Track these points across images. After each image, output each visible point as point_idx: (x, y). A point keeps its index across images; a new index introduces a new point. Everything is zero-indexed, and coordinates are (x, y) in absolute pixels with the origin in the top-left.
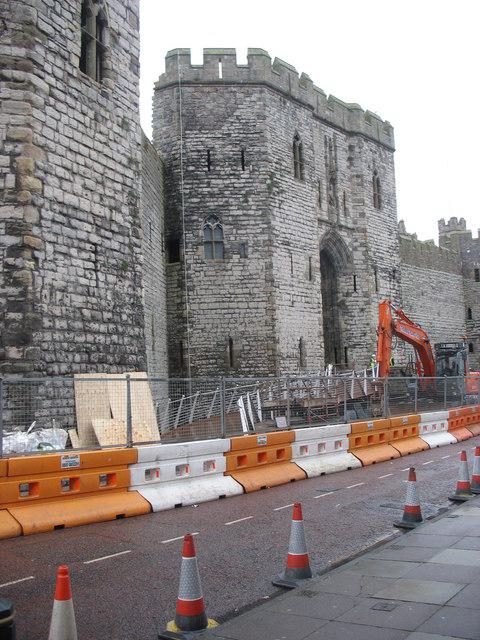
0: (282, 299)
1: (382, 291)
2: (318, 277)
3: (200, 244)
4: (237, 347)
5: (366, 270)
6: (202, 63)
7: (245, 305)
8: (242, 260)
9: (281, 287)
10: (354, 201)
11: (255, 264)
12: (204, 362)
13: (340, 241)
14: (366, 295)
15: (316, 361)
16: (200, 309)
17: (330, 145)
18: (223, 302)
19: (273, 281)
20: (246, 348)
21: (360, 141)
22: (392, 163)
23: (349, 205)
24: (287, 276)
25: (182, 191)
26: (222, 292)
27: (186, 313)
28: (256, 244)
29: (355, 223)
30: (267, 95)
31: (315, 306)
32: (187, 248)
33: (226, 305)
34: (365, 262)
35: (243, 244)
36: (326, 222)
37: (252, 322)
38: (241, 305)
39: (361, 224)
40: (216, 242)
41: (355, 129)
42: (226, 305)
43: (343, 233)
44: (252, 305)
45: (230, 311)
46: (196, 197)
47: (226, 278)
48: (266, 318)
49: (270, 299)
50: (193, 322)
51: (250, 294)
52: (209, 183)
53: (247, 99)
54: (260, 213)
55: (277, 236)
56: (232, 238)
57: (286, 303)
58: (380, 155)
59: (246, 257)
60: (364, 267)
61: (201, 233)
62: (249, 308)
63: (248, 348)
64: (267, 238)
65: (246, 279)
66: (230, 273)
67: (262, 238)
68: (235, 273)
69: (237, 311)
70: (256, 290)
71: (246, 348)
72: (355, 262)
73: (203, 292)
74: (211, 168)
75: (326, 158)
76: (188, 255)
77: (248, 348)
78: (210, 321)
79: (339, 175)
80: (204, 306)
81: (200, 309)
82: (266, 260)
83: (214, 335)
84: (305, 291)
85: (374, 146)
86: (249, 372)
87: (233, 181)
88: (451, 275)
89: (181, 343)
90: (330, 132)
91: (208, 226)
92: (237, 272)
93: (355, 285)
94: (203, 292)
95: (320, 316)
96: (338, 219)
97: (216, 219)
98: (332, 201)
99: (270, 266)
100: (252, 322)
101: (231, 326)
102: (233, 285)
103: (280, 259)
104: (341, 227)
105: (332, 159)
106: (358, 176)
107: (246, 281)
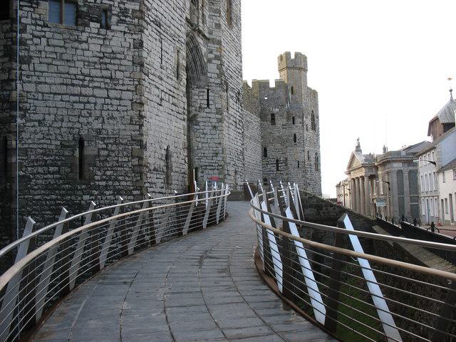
0: (151, 94)
1: (231, 111)
4: (90, 151)
7: (104, 93)
8: (103, 31)
9: (151, 76)
10: (211, 9)
11: (119, 40)
12: (40, 170)
14: (219, 111)
16: (37, 92)
18: (73, 85)
19: (142, 65)
23: (207, 13)
24: (157, 65)
26: (73, 71)
28: (124, 12)
29: (210, 33)
31: (181, 110)
33: (77, 90)
35: (105, 11)
37: (112, 118)
38: (97, 92)
42: (77, 90)
43: (200, 40)
44: (113, 94)
45: (82, 99)
47: (79, 52)
48: (131, 113)
49: (138, 88)
50: (27, 110)
51: (111, 78)
55: (148, 9)
60: (218, 81)
62: (108, 97)
63: (106, 153)
64: (137, 8)
65: (106, 58)
66: (84, 46)
68: (92, 47)
70: (119, 75)
72: (209, 75)
73: (44, 68)
77: (106, 153)
78: (53, 111)
80: (45, 88)
81: (37, 92)
82: (135, 37)
83: (58, 131)
84: (172, 89)
86: (106, 187)
89: (6, 140)
93: (208, 100)
94: (44, 68)
95: (185, 124)
100: (112, 118)
101: (82, 120)
104: (200, 32)
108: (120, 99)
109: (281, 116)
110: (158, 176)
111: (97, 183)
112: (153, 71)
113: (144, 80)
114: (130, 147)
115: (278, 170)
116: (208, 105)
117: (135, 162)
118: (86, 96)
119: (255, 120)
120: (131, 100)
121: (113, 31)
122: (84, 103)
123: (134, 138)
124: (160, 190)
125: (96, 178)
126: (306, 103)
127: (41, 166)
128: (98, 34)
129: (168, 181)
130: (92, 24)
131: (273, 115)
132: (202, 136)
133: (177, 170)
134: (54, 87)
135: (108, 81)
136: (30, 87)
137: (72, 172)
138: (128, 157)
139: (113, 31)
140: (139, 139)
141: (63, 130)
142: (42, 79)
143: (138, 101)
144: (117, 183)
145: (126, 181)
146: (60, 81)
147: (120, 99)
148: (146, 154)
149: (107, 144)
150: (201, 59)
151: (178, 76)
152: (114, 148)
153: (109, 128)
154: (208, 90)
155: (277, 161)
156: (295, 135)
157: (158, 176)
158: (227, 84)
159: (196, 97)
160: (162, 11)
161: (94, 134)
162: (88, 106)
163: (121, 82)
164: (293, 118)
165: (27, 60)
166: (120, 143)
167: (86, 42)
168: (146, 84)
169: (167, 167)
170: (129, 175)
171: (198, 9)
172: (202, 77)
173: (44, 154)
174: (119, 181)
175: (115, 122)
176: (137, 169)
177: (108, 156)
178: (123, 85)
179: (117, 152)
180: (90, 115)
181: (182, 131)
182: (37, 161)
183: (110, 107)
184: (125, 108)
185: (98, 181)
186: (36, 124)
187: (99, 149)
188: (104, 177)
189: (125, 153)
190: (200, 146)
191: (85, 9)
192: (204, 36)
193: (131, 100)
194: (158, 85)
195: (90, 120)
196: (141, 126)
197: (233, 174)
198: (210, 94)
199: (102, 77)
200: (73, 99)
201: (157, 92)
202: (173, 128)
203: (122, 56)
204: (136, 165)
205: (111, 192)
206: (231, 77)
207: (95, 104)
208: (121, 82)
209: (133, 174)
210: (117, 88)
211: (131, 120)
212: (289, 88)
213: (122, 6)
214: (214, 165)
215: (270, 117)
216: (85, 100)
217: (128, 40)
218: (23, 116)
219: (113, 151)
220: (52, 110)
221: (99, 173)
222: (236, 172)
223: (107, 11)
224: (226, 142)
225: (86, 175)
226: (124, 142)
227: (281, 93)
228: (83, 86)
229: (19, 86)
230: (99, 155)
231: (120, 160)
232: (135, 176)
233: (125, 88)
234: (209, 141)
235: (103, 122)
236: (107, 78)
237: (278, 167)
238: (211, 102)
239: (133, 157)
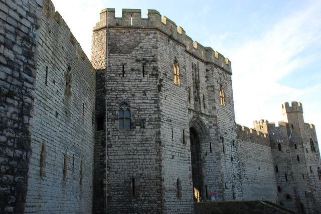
0: (166, 154)
1: (227, 152)
2: (188, 142)
3: (117, 119)
4: (137, 184)
5: (217, 140)
6: (121, 17)
7: (143, 157)
10: (209, 100)
11: (149, 132)
12: (116, 193)
13: (201, 122)
17: (195, 68)
18: (129, 155)
20: (143, 184)
21: (212, 67)
22: (231, 81)
23: (207, 102)
24: (170, 140)
25: (107, 88)
26: (129, 149)
27: (106, 161)
29: (210, 112)
30: (159, 35)
31: (187, 159)
32: (108, 121)
33: (131, 157)
34: (216, 135)
35: (143, 120)
36: (193, 110)
39: (213, 113)
40: (126, 119)
41: (209, 60)
42: (131, 157)
43: (203, 118)
44: (147, 157)
46: (115, 91)
49: (159, 154)
50: (110, 167)
51: (146, 150)
52: (123, 84)
53: (147, 37)
54: (153, 101)
55: (163, 116)
56: (136, 116)
57: (168, 156)
58: (224, 76)
59: (144, 128)
60: (216, 138)
61: (117, 113)
63: (144, 184)
64: (157, 116)
66: (134, 137)
67: (154, 116)
68: (137, 137)
69: (138, 160)
70: (150, 148)
71: (143, 184)
73: (117, 149)
74: (125, 75)
75: (193, 75)
76: (109, 126)
77: (144, 184)
78: (121, 167)
79: (201, 85)
80: (117, 157)
82: (156, 130)
84: (180, 149)
85: (220, 71)
87: (137, 83)
88: (265, 147)
90: (195, 61)
91: (122, 109)
92: (138, 137)
93: (211, 149)
94: (117, 149)
95: (190, 165)
96: (200, 109)
97: (127, 104)
98: (197, 99)
99: (159, 133)
101: (133, 170)
102: (136, 145)
103: (165, 130)
104: (202, 114)
105: (196, 75)
106: (211, 86)
107: (144, 142)
109: (285, 144)
112: (167, 144)
116: (211, 151)
117: (158, 187)
120: (156, 159)
121: (146, 129)
122: (135, 162)
124: (174, 200)
126: (303, 134)
127: (116, 191)
128: (140, 131)
129: (179, 195)
130: (137, 127)
131: (279, 145)
134: (122, 157)
136: (112, 157)
137: (129, 193)
139: (146, 129)
140: (160, 176)
141: (126, 175)
142: (116, 154)
146: (123, 153)
148: (163, 183)
150: (205, 127)
151: (184, 142)
154: (210, 143)
155: (286, 174)
156: (298, 156)
159: (204, 148)
160: (171, 114)
163: (151, 151)
164: (295, 145)
165: (110, 146)
167: (135, 135)
168: (163, 150)
171: (200, 102)
173: (117, 186)
178: (152, 152)
181: (188, 169)
182: (114, 189)
186: (114, 173)
191: (133, 121)
192: (205, 115)
193: (156, 159)
196: (161, 170)
197: (231, 188)
200: (130, 161)
201: (170, 153)
202: (181, 169)
203: (151, 140)
206: (226, 133)
208: (151, 151)
212: (290, 125)
213: (150, 117)
215: (277, 145)
217: (153, 132)
218: (109, 170)
220: (121, 167)
223: (143, 120)
224: (223, 170)
227: (285, 131)
228: (135, 155)
229: (107, 158)
233: (153, 154)
239: (157, 185)
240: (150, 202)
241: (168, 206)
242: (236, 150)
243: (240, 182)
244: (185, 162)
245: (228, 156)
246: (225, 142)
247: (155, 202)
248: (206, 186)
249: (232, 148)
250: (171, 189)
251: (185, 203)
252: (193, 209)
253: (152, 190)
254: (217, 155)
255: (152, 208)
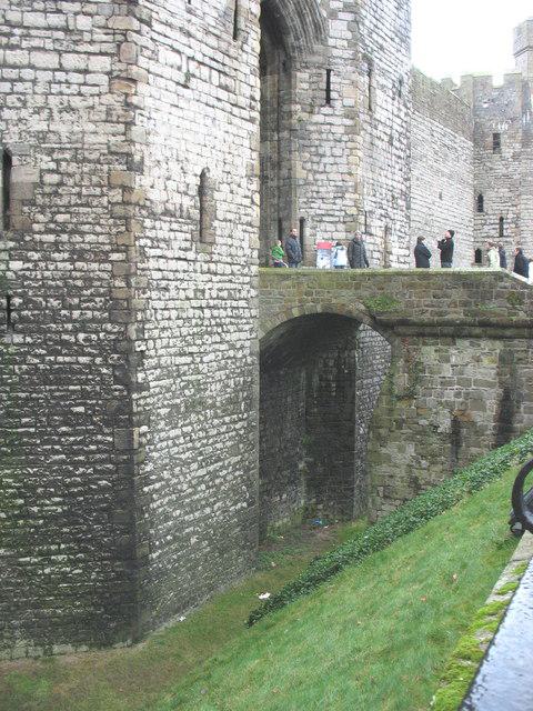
7: (51, 60)
9: (156, 26)
15: (238, 233)
20: (49, 178)
31: (243, 101)
34: (352, 44)
37: (70, 109)
38: (39, 59)
44: (70, 61)
48: (108, 99)
51: (66, 30)
57: (168, 72)
63: (55, 178)
69: (28, 74)
71: (49, 178)
72: (331, 42)
77: (55, 178)
84: (219, 57)
86: (56, 246)
93: (328, 90)
95: (255, 128)
100: (70, 109)
108: (86, 72)
110: (175, 226)
111: (37, 237)
112: (164, 16)
113: (138, 32)
114: (106, 167)
115: (501, 235)
117: (116, 195)
118: (14, 67)
119: (464, 145)
120: (109, 74)
122: (12, 81)
123: (113, 149)
124: (182, 254)
125: (36, 227)
131: (496, 136)
132: (315, 159)
133: (229, 216)
135: (60, 35)
138: (101, 186)
140: (125, 150)
143: (124, 75)
144: (77, 238)
145: (98, 234)
147: (86, 72)
149: (57, 162)
152: (73, 167)
153: (63, 129)
154: (329, 72)
155: (501, 219)
157: (175, 226)
158: (370, 63)
161: (33, 141)
162: (19, 87)
163: (87, 37)
166: (85, 160)
169: (202, 210)
170: (102, 222)
172: (317, 47)
174: (82, 234)
175: (74, 117)
176: (119, 210)
177: (60, 184)
178: (92, 42)
179: (77, 177)
180: (24, 103)
181: (246, 143)
183: (63, 88)
184: (95, 90)
185: (40, 233)
187: (41, 171)
188: (52, 226)
189: (95, 179)
190: (311, 178)
193: (109, 74)
194: (176, 46)
195: (24, 113)
196: (129, 124)
197: (380, 233)
198: (332, 79)
199: (49, 28)
201: (174, 59)
204: (117, 203)
205: (66, 255)
206: (382, 48)
207: (34, 82)
208: (87, 37)
209: (111, 221)
210: (79, 48)
211: (108, 113)
214: (337, 213)
216: (13, 74)
219: (70, 175)
221: (40, 217)
222: (387, 230)
225: (17, 220)
226: (94, 156)
227: (514, 97)
230: (42, 184)
231: (84, 191)
232: (115, 225)
234: (328, 168)
235: (50, 118)
236: (57, 29)
237: (501, 229)
238: (334, 95)
239: (111, 187)
240: (78, 255)
241: (157, 275)
242: (406, 114)
243: (408, 217)
244: (236, 111)
245: (380, 127)
246: (378, 79)
247: (102, 257)
248: (302, 221)
249: (396, 103)
250: (171, 207)
251: (228, 269)
252: (253, 293)
253: (87, 205)
254: (347, 117)
255: (88, 281)
